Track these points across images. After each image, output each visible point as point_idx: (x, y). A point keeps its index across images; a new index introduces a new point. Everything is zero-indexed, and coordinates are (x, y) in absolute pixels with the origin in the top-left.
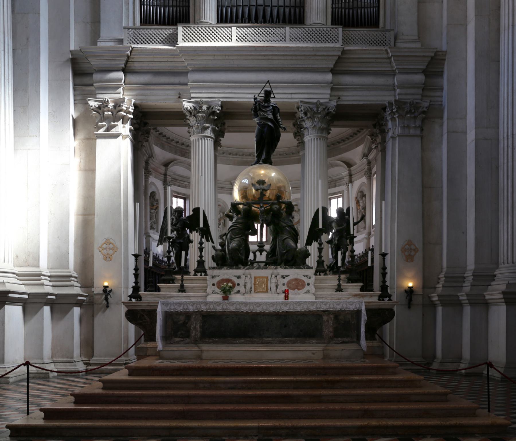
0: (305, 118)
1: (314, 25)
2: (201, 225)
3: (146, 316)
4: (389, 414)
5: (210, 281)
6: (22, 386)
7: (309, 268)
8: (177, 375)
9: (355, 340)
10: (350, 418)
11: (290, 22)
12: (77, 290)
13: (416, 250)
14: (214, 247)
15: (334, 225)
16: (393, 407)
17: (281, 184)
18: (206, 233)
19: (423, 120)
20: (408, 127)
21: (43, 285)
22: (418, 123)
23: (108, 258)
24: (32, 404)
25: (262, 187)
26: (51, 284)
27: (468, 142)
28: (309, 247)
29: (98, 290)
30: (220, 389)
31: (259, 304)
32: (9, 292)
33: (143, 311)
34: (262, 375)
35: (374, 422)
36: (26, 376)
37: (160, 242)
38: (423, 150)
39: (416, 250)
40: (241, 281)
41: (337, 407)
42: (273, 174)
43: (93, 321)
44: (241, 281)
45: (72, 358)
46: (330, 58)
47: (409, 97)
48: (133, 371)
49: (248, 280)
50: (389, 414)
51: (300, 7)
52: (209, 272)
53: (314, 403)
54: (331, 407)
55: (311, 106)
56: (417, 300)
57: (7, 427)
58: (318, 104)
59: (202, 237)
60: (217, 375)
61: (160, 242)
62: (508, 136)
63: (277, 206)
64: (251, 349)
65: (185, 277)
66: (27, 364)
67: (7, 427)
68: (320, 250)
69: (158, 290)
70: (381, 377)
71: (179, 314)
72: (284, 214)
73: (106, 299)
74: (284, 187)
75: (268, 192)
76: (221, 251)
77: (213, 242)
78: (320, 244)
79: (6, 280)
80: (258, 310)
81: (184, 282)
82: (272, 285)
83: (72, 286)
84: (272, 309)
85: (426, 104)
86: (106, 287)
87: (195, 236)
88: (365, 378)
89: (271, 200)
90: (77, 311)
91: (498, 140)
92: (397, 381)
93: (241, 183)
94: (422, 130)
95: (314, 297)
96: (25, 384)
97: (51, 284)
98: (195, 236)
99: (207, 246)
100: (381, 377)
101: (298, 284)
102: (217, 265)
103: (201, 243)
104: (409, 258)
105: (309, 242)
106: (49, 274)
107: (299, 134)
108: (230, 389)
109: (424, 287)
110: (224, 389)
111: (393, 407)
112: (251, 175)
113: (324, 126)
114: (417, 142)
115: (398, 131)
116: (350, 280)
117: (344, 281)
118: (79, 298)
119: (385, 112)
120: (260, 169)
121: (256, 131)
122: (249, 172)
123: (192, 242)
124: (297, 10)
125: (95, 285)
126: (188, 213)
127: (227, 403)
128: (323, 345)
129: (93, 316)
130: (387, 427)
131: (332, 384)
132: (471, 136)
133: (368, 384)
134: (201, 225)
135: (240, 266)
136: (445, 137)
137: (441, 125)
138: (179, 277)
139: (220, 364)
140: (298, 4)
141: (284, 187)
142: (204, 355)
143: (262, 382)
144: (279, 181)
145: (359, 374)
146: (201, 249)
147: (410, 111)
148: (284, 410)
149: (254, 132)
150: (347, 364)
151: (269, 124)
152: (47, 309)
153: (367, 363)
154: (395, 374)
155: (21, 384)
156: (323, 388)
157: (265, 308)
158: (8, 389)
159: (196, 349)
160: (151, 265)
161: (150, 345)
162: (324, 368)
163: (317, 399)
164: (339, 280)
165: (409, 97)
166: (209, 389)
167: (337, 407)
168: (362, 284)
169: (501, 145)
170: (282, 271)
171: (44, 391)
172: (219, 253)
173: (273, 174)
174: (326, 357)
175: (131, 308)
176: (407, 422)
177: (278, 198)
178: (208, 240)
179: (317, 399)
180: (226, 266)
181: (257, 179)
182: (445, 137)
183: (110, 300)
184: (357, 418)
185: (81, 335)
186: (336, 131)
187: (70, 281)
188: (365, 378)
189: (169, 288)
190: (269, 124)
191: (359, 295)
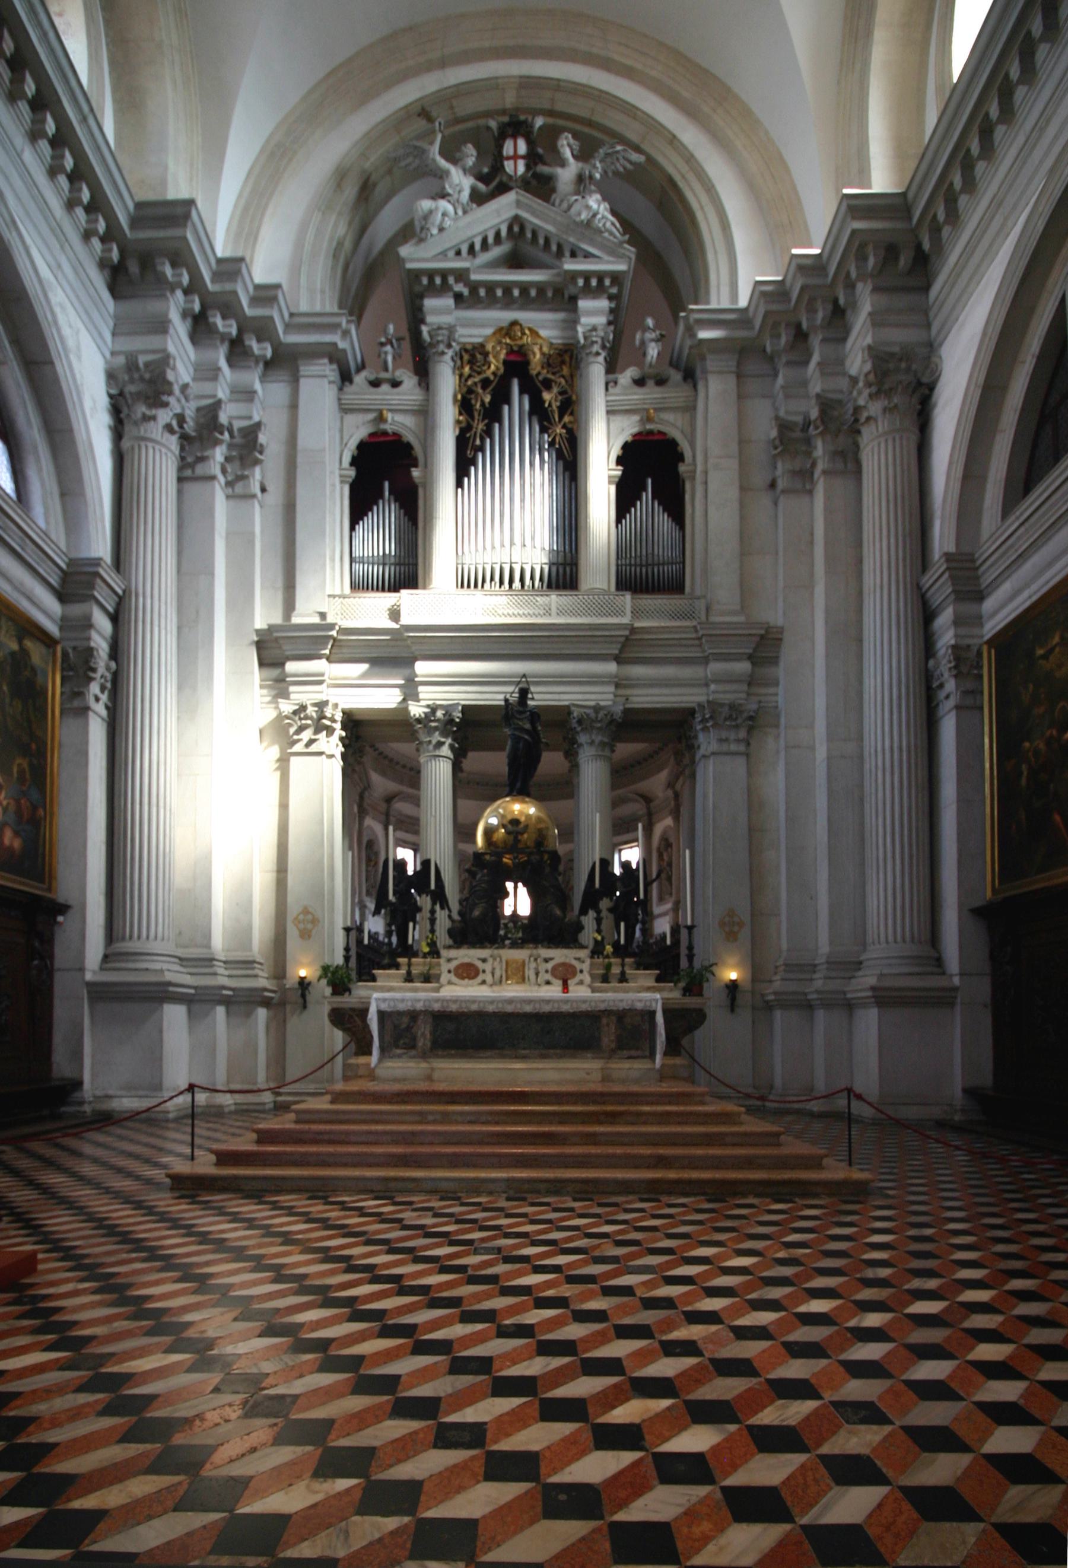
0: (579, 729)
1: (592, 592)
2: (433, 886)
3: (356, 1018)
4: (692, 1163)
5: (445, 966)
6: (186, 1125)
7: (582, 947)
8: (398, 1103)
9: (647, 1053)
10: (637, 1167)
11: (558, 588)
12: (263, 982)
14: (450, 917)
15: (619, 884)
16: (699, 1152)
17: (542, 826)
18: (439, 896)
19: (750, 730)
20: (727, 740)
21: (215, 974)
23: (305, 935)
24: (200, 1147)
25: (515, 828)
26: (227, 973)
27: (817, 763)
28: (583, 918)
29: (291, 982)
30: (457, 1123)
31: (510, 1001)
32: (170, 984)
33: (353, 1009)
34: (514, 1103)
35: (672, 1175)
36: (190, 1111)
37: (376, 912)
38: (749, 774)
41: (619, 1151)
42: (532, 811)
43: (285, 1029)
45: (255, 1083)
46: (614, 639)
47: (728, 696)
48: (338, 1097)
49: (496, 964)
50: (692, 1163)
51: (571, 565)
52: (444, 953)
53: (586, 1144)
54: (610, 1150)
55: (588, 711)
57: (168, 1176)
58: (597, 709)
59: (434, 903)
60: (453, 1102)
61: (376, 912)
62: (876, 751)
63: (537, 857)
64: (501, 1066)
65: (414, 960)
66: (191, 1088)
67: (168, 1176)
68: (599, 920)
69: (374, 979)
70: (682, 1108)
71: (400, 1014)
72: (547, 870)
73: (303, 996)
74: (547, 828)
75: (525, 836)
76: (460, 922)
77: (450, 910)
78: (599, 912)
79: (165, 966)
80: (509, 1009)
81: (412, 968)
82: (530, 973)
83: (256, 976)
84: (528, 1009)
86: (302, 979)
87: (424, 902)
88: (660, 1108)
89: (528, 847)
90: (262, 1013)
91: (861, 757)
92: (706, 1115)
93: (487, 823)
94: (748, 744)
95: (589, 990)
96: (190, 1121)
97: (227, 973)
98: (424, 902)
99: (441, 915)
100: (682, 1108)
102: (455, 942)
103: (433, 912)
105: (583, 911)
106: (224, 959)
107: (571, 754)
108: (470, 1122)
110: (463, 1123)
111: (699, 1152)
112: (501, 811)
113: (606, 740)
114: (741, 761)
115: (714, 746)
116: (638, 966)
117: (631, 968)
118: (267, 994)
119: (694, 718)
120: (514, 801)
121: (508, 748)
122: (499, 807)
123: (419, 910)
124: (568, 569)
125: (288, 975)
127: (466, 1144)
128: (602, 1061)
129: (285, 1021)
130: (690, 1182)
131: (612, 1118)
132: (821, 753)
133: (665, 1118)
134: (433, 886)
135: (487, 944)
136: (782, 754)
137: (777, 737)
138: (402, 960)
139: (456, 1088)
140: (568, 560)
141: (547, 828)
142: (436, 1075)
143: (514, 1113)
144: (539, 820)
145: (652, 1104)
146: (433, 921)
147: (731, 716)
148: (544, 1155)
149: (503, 749)
150: (635, 1088)
151: (526, 737)
152: (221, 1010)
153: (665, 1087)
154: (703, 1103)
155: (185, 1121)
156: (600, 1123)
157: (519, 1006)
158: (168, 1129)
159: (424, 1065)
160: (366, 942)
161: (362, 1060)
162: (602, 1094)
163: (592, 1139)
164: (623, 965)
165: (728, 696)
166: (442, 1123)
167: (619, 1151)
168: (658, 972)
169: (867, 766)
171: (215, 1130)
172: (458, 925)
173: (532, 811)
174: (606, 1079)
175: (335, 1006)
176: (718, 1175)
178: (442, 908)
179: (592, 1139)
180: (467, 943)
181: (509, 817)
182: (782, 754)
183: (309, 998)
184: (648, 1167)
185: (267, 1050)
186: (626, 749)
187: (254, 968)
188: (660, 1108)
189: (389, 976)
190: (526, 737)
191: (653, 987)
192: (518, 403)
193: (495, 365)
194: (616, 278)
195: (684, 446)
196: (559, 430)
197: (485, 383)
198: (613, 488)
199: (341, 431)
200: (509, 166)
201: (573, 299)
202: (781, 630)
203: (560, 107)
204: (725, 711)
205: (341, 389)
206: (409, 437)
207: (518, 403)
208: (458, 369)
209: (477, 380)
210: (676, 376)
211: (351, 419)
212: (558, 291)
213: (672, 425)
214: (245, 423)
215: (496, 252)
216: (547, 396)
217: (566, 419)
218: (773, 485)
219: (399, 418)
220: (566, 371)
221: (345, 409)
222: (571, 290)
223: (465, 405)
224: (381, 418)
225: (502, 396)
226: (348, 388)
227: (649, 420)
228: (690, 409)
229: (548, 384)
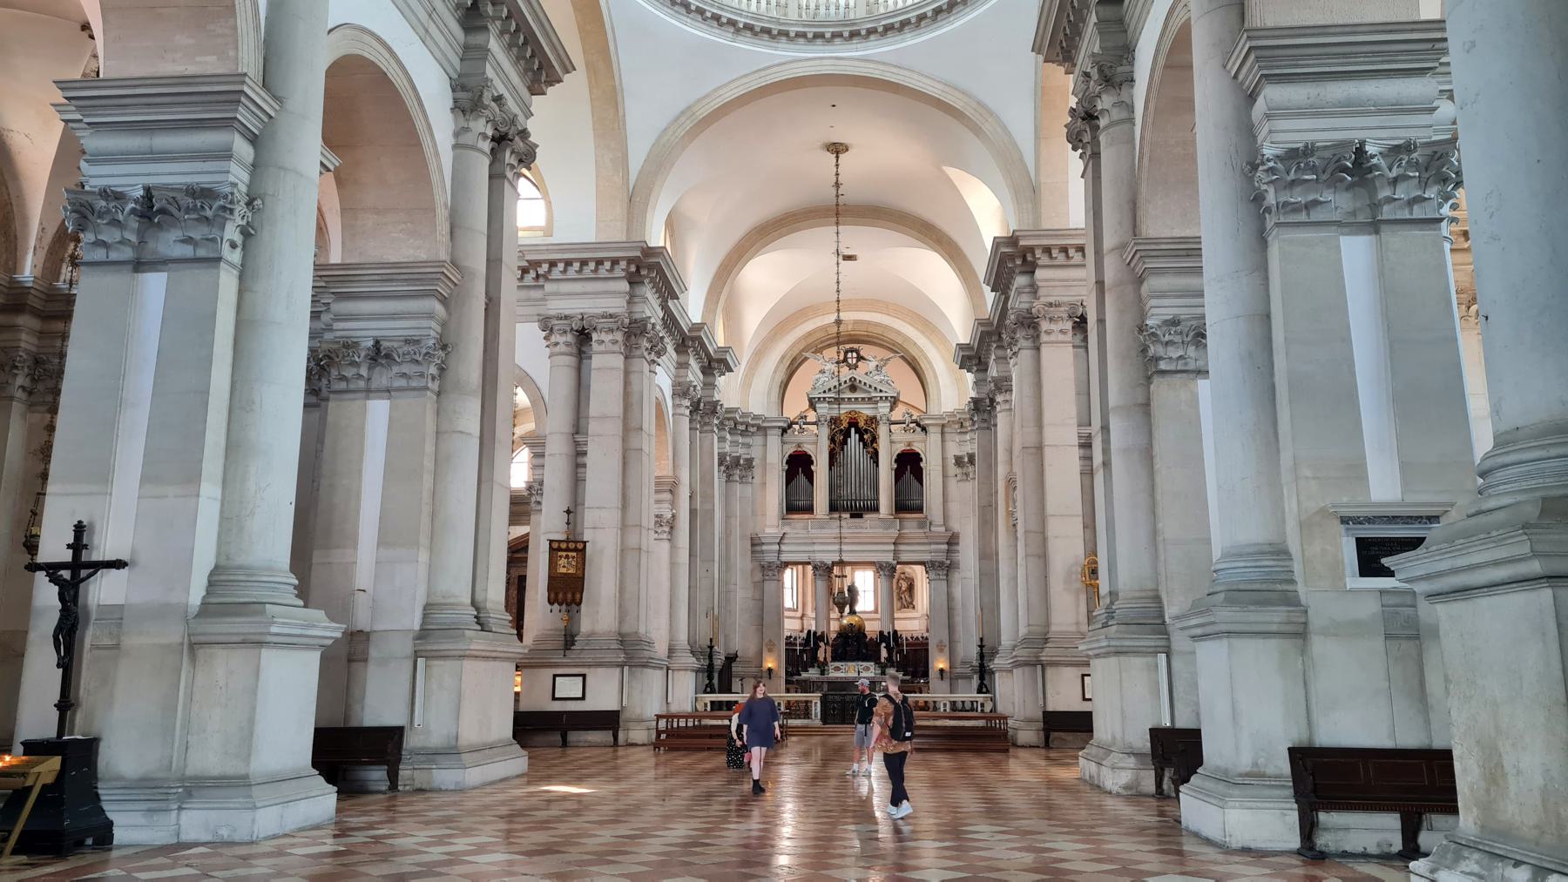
13: (945, 646)
22: (945, 572)
39: (945, 646)
40: (843, 668)
44: (843, 668)
56: (946, 675)
85: (948, 562)
101: (867, 669)
104: (941, 651)
109: (950, 668)
126: (819, 634)
170: (860, 663)
177: (859, 630)
192: (854, 437)
193: (845, 425)
194: (891, 397)
195: (922, 456)
196: (871, 450)
197: (841, 430)
198: (893, 472)
199: (782, 451)
200: (850, 361)
201: (876, 403)
202: (958, 533)
203: (869, 330)
204: (937, 564)
205: (782, 435)
206: (810, 453)
207: (854, 437)
208: (830, 426)
209: (837, 429)
210: (919, 429)
211: (786, 446)
212: (870, 399)
213: (917, 448)
214: (749, 457)
215: (844, 386)
216: (865, 437)
217: (875, 445)
218: (956, 476)
219: (809, 446)
220: (874, 426)
221: (783, 443)
222: (875, 399)
223: (832, 440)
224: (799, 447)
225: (847, 435)
226: (785, 435)
227: (909, 446)
228: (925, 441)
229: (866, 431)
